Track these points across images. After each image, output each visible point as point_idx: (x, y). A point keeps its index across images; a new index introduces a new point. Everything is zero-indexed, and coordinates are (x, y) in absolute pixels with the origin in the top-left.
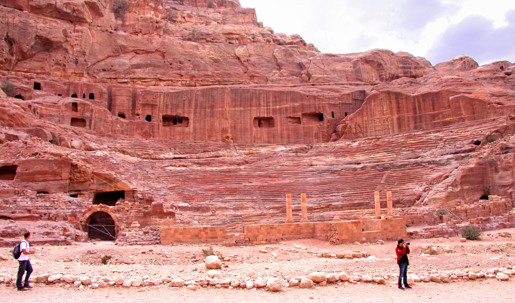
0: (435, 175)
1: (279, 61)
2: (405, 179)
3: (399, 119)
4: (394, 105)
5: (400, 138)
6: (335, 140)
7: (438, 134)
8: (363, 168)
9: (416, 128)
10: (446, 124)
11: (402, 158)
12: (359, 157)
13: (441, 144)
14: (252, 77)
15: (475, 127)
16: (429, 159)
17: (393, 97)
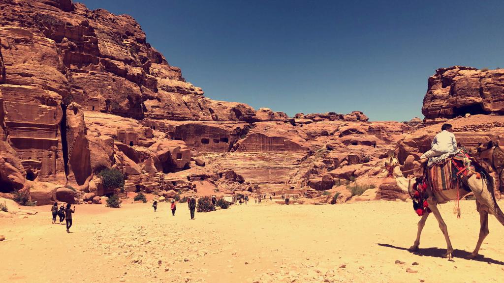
0: (291, 173)
1: (202, 107)
2: (279, 174)
3: (263, 146)
4: (261, 139)
5: (266, 154)
6: (233, 152)
7: (280, 155)
8: (258, 167)
9: (269, 150)
10: (282, 150)
11: (272, 164)
12: (253, 162)
13: (285, 160)
14: (194, 116)
15: (295, 154)
16: (284, 166)
17: (261, 137)
